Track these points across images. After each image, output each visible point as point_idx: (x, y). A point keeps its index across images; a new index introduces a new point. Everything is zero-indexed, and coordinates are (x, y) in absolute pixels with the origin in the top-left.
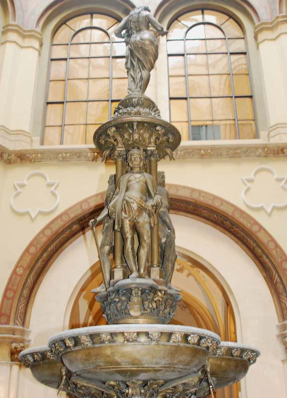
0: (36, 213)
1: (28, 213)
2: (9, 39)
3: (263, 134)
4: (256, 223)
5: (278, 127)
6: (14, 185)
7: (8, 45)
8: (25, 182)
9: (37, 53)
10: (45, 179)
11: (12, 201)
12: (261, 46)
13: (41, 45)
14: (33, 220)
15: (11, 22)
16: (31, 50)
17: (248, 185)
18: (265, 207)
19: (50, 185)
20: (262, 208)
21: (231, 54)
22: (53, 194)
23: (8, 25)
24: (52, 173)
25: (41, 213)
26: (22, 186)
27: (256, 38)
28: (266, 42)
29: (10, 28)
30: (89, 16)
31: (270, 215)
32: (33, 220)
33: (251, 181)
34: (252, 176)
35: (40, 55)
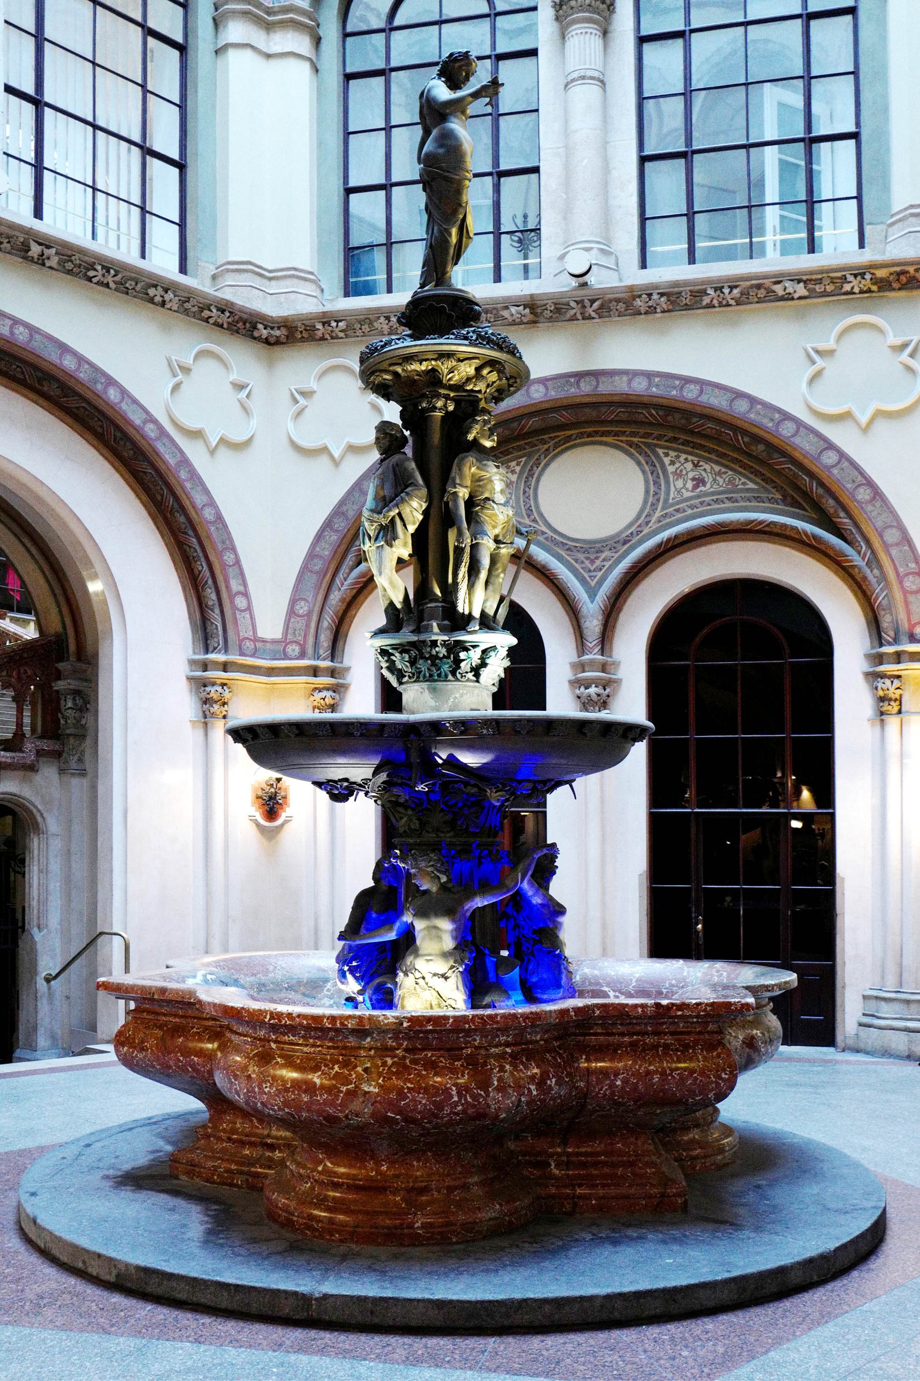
0: (343, 446)
1: (324, 450)
4: (830, 446)
5: (270, 271)
6: (292, 395)
11: (290, 425)
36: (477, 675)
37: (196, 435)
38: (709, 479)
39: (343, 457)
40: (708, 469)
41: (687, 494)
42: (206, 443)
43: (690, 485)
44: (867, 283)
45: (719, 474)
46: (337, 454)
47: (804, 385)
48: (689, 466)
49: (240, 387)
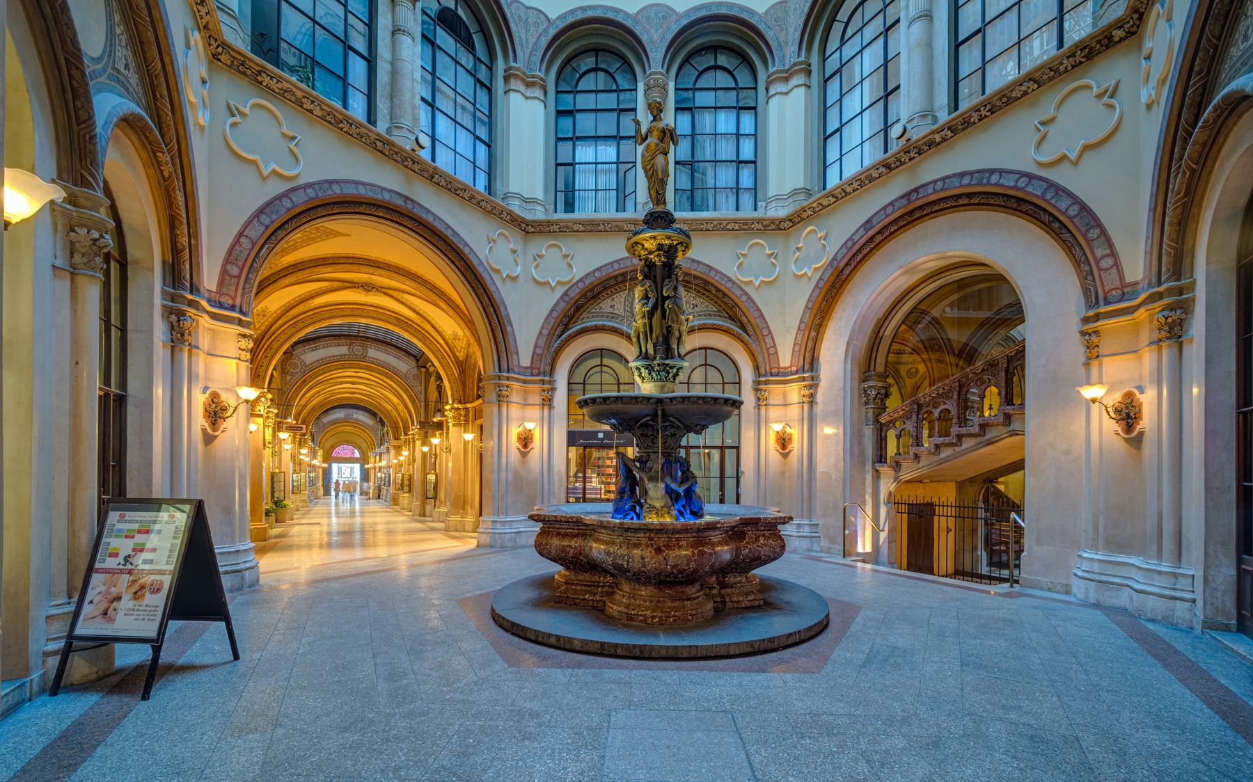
1: (548, 283)
2: (512, 87)
3: (761, 204)
7: (512, 94)
8: (544, 252)
9: (542, 105)
10: (561, 249)
11: (533, 271)
12: (771, 101)
13: (546, 94)
14: (553, 289)
15: (513, 64)
16: (537, 102)
17: (742, 259)
18: (754, 281)
19: (566, 256)
20: (751, 282)
21: (741, 108)
22: (570, 266)
23: (510, 68)
24: (569, 245)
25: (559, 283)
26: (541, 256)
27: (767, 90)
28: (777, 97)
29: (512, 72)
30: (594, 53)
31: (757, 289)
32: (553, 289)
33: (744, 256)
34: (746, 252)
35: (545, 107)
36: (674, 379)
37: (498, 271)
38: (699, 304)
39: (556, 285)
40: (699, 301)
41: (691, 311)
42: (501, 276)
43: (692, 306)
44: (760, 226)
45: (702, 303)
46: (553, 284)
47: (736, 268)
48: (692, 298)
49: (514, 252)
